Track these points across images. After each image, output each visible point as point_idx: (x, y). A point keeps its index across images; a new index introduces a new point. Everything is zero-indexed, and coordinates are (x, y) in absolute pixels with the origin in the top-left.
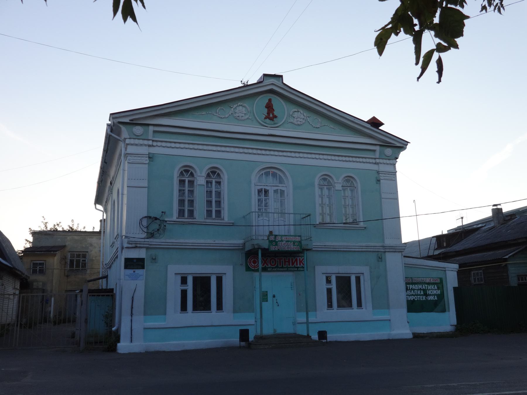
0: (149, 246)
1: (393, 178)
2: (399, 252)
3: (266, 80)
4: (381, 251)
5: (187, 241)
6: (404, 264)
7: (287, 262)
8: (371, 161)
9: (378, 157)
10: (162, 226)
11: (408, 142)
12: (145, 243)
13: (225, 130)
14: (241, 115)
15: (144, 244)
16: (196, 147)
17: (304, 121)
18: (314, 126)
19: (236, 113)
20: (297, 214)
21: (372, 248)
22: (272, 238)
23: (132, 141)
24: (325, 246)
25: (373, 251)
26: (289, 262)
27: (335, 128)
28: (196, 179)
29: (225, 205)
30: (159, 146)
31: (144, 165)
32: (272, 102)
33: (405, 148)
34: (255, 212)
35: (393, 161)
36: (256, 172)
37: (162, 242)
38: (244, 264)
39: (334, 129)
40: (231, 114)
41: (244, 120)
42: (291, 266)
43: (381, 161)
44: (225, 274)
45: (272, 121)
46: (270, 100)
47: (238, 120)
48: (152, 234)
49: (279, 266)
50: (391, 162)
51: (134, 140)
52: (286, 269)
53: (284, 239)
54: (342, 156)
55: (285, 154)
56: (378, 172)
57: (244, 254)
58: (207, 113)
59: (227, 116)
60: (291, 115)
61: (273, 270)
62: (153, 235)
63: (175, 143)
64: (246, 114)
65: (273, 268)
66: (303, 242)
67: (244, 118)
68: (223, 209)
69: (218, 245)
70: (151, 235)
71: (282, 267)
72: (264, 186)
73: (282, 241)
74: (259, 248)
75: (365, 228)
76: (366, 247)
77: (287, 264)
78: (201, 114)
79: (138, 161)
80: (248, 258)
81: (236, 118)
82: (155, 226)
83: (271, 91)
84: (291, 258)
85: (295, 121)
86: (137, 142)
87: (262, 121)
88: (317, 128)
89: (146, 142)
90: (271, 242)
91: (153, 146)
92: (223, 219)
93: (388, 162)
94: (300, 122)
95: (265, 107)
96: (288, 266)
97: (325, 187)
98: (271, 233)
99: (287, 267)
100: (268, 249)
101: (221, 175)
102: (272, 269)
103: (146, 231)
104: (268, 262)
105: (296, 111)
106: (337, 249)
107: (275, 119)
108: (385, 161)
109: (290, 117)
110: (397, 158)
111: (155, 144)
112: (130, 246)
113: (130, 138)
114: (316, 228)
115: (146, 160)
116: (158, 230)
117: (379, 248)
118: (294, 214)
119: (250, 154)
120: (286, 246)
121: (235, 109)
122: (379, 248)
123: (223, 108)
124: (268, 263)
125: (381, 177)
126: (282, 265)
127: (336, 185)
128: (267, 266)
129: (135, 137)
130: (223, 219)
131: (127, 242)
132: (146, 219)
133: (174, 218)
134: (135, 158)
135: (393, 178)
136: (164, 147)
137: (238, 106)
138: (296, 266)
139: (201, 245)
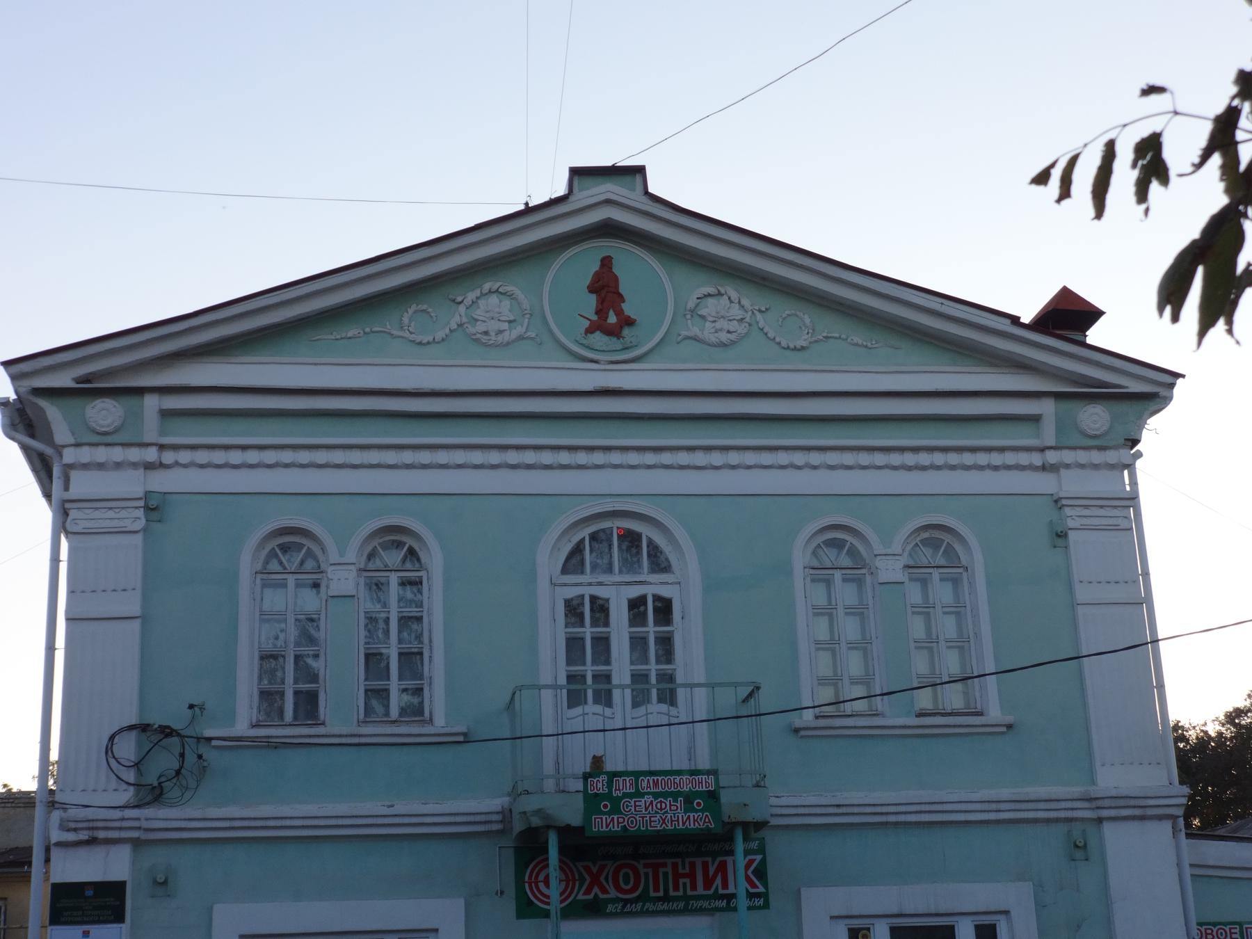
0: (144, 836)
1: (1119, 521)
2: (1160, 818)
3: (580, 190)
4: (1083, 820)
5: (286, 810)
6: (1191, 865)
7: (684, 876)
8: (1024, 459)
9: (1052, 443)
10: (191, 758)
11: (1178, 376)
12: (125, 824)
13: (427, 385)
14: (493, 326)
15: (120, 829)
16: (321, 457)
17: (742, 329)
18: (784, 344)
19: (477, 320)
20: (721, 685)
21: (1042, 805)
22: (600, 784)
23: (85, 454)
24: (838, 806)
25: (1048, 821)
26: (692, 876)
27: (869, 344)
28: (324, 574)
29: (436, 667)
30: (185, 466)
31: (125, 539)
32: (614, 270)
33: (1167, 400)
34: (555, 687)
35: (1124, 455)
36: (555, 535)
37: (190, 820)
38: (511, 891)
39: (866, 347)
40: (456, 327)
41: (508, 344)
42: (700, 890)
43: (1068, 456)
44: (436, 930)
45: (614, 339)
46: (606, 262)
47: (486, 345)
48: (157, 792)
49: (652, 894)
50: (1111, 457)
51: (93, 449)
52: (682, 905)
53: (645, 784)
54: (902, 450)
55: (666, 458)
56: (1056, 502)
57: (513, 849)
58: (368, 330)
59: (440, 335)
60: (692, 311)
61: (628, 908)
62: (161, 794)
63: (244, 448)
64: (514, 321)
65: (626, 902)
66: (725, 797)
67: (506, 337)
68: (431, 684)
69: (406, 820)
70: (152, 794)
71: (666, 898)
72: (590, 584)
73: (639, 794)
74: (548, 827)
75: (1009, 727)
76: (1013, 806)
77: (685, 884)
78: (344, 335)
79: (107, 524)
80: (527, 867)
81: (477, 340)
82: (164, 762)
83: (608, 229)
84: (699, 862)
85: (707, 332)
86: (101, 454)
87: (577, 341)
88: (795, 349)
89: (134, 454)
90: (592, 802)
91: (162, 465)
92: (431, 721)
93: (1096, 457)
94: (729, 332)
95: (587, 290)
96: (689, 893)
97: (836, 576)
98: (597, 762)
99: (686, 898)
100: (580, 830)
101: (422, 555)
102: (624, 907)
103: (132, 780)
104: (607, 882)
105: (709, 295)
106: (892, 819)
107: (626, 331)
108: (1082, 456)
109: (689, 317)
110: (1135, 442)
111: (168, 457)
112: (71, 837)
113: (77, 445)
114: (802, 737)
115: (135, 518)
116: (178, 773)
117: (1069, 805)
118: (711, 686)
119: (529, 467)
120: (657, 813)
121: (471, 306)
122: (1069, 805)
123: (425, 307)
124: (605, 883)
125: (1069, 520)
126: (666, 891)
127: (879, 563)
128: (602, 896)
129: (96, 439)
130: (431, 719)
131: (60, 825)
132: (134, 733)
133: (241, 727)
134: (97, 514)
135: (1119, 521)
136: (202, 466)
137: (482, 295)
138: (721, 891)
139: (340, 822)
